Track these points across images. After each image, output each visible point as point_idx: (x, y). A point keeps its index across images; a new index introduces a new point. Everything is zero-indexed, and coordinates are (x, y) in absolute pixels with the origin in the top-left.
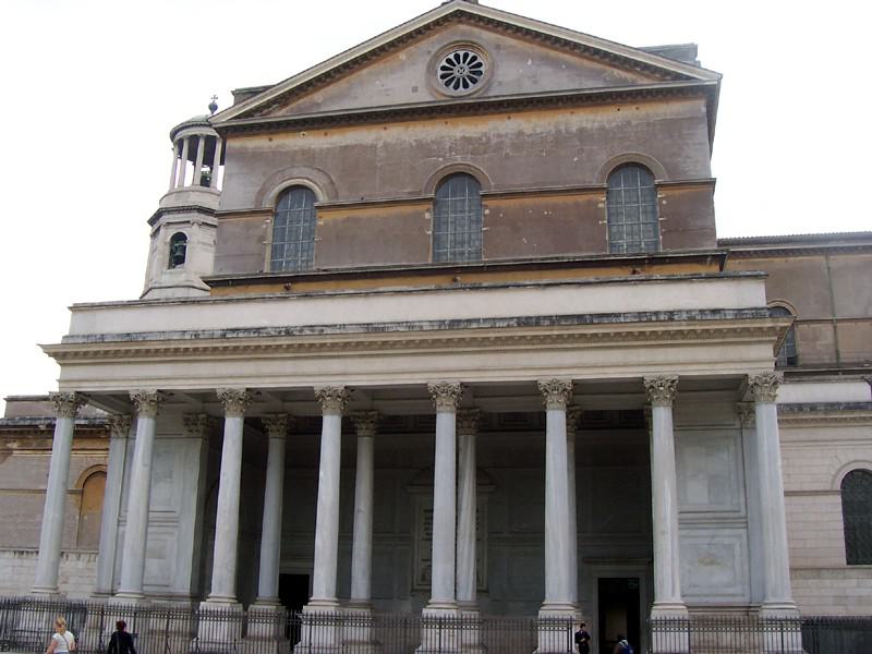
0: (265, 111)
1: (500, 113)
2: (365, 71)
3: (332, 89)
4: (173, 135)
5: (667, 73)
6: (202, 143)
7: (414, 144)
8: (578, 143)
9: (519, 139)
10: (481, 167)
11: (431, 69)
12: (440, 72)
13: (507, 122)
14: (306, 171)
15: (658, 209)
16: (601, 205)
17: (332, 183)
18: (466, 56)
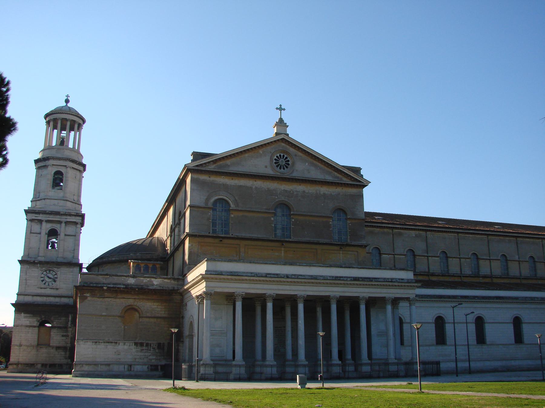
0: (207, 164)
3: (234, 160)
5: (356, 179)
15: (348, 227)
16: (330, 223)
17: (236, 200)
18: (284, 156)
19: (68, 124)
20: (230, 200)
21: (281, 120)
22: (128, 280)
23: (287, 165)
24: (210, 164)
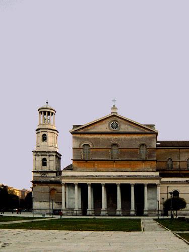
9: (125, 140)
11: (109, 125)
19: (47, 113)
21: (114, 106)
23: (117, 126)
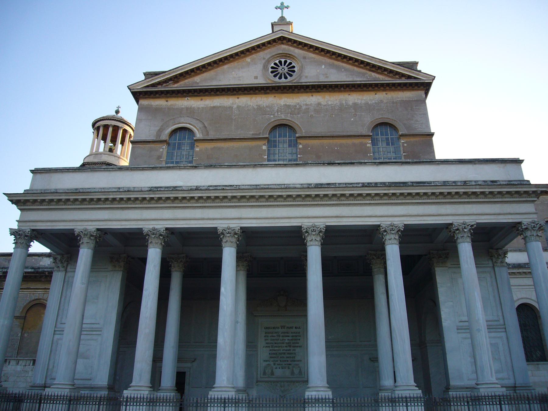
1: (307, 92)
2: (226, 67)
3: (206, 75)
4: (93, 125)
6: (111, 129)
7: (256, 107)
8: (353, 111)
9: (319, 108)
10: (297, 121)
11: (265, 67)
12: (270, 70)
13: (311, 98)
14: (189, 120)
16: (368, 145)
17: (205, 127)
18: (285, 62)
20: (195, 127)
22: (41, 261)
24: (168, 84)
